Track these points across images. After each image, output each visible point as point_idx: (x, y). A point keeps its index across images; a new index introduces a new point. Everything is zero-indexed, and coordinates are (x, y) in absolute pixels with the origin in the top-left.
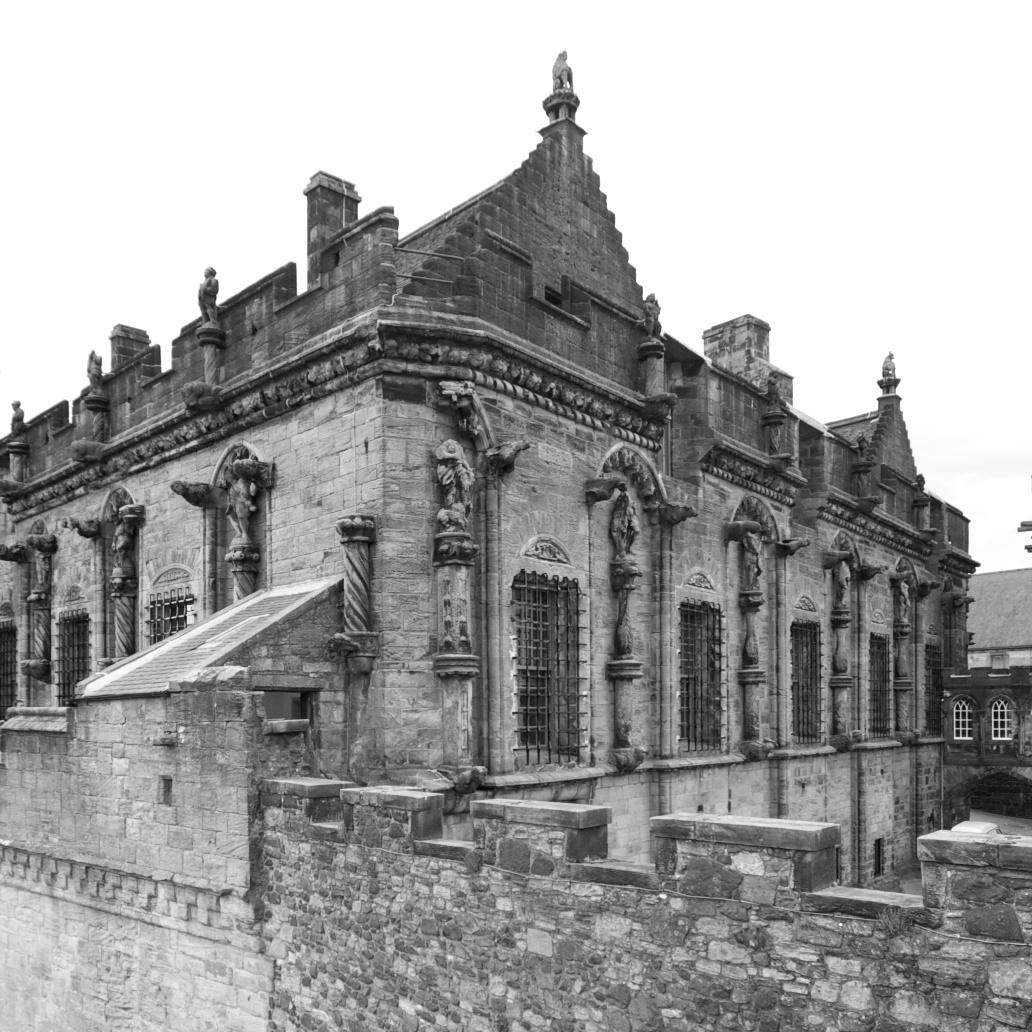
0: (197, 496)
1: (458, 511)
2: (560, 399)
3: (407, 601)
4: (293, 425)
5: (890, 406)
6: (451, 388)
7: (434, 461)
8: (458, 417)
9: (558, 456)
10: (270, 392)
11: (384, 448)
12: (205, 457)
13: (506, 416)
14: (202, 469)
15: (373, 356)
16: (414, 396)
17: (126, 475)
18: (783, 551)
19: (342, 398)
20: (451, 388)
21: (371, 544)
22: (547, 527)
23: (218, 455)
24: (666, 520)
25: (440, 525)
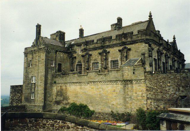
0: (120, 51)
1: (151, 53)
2: (155, 43)
3: (147, 60)
4: (133, 45)
5: (175, 41)
6: (150, 43)
7: (149, 49)
8: (150, 45)
9: (156, 48)
10: (131, 42)
11: (145, 48)
12: (120, 47)
13: (153, 46)
14: (121, 48)
15: (144, 40)
16: (147, 44)
17: (106, 48)
18: (169, 57)
19: (140, 44)
20: (150, 43)
21: (144, 55)
22: (155, 55)
23: (122, 47)
24: (162, 54)
25: (149, 54)
